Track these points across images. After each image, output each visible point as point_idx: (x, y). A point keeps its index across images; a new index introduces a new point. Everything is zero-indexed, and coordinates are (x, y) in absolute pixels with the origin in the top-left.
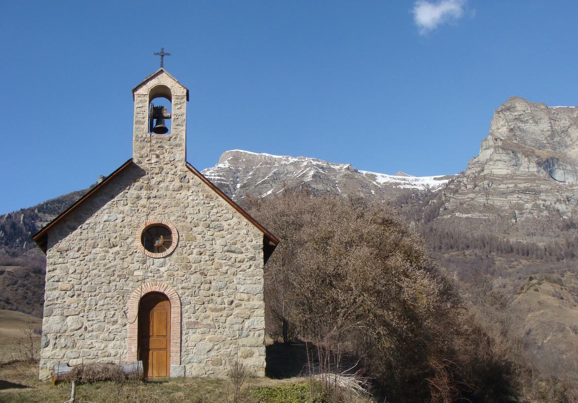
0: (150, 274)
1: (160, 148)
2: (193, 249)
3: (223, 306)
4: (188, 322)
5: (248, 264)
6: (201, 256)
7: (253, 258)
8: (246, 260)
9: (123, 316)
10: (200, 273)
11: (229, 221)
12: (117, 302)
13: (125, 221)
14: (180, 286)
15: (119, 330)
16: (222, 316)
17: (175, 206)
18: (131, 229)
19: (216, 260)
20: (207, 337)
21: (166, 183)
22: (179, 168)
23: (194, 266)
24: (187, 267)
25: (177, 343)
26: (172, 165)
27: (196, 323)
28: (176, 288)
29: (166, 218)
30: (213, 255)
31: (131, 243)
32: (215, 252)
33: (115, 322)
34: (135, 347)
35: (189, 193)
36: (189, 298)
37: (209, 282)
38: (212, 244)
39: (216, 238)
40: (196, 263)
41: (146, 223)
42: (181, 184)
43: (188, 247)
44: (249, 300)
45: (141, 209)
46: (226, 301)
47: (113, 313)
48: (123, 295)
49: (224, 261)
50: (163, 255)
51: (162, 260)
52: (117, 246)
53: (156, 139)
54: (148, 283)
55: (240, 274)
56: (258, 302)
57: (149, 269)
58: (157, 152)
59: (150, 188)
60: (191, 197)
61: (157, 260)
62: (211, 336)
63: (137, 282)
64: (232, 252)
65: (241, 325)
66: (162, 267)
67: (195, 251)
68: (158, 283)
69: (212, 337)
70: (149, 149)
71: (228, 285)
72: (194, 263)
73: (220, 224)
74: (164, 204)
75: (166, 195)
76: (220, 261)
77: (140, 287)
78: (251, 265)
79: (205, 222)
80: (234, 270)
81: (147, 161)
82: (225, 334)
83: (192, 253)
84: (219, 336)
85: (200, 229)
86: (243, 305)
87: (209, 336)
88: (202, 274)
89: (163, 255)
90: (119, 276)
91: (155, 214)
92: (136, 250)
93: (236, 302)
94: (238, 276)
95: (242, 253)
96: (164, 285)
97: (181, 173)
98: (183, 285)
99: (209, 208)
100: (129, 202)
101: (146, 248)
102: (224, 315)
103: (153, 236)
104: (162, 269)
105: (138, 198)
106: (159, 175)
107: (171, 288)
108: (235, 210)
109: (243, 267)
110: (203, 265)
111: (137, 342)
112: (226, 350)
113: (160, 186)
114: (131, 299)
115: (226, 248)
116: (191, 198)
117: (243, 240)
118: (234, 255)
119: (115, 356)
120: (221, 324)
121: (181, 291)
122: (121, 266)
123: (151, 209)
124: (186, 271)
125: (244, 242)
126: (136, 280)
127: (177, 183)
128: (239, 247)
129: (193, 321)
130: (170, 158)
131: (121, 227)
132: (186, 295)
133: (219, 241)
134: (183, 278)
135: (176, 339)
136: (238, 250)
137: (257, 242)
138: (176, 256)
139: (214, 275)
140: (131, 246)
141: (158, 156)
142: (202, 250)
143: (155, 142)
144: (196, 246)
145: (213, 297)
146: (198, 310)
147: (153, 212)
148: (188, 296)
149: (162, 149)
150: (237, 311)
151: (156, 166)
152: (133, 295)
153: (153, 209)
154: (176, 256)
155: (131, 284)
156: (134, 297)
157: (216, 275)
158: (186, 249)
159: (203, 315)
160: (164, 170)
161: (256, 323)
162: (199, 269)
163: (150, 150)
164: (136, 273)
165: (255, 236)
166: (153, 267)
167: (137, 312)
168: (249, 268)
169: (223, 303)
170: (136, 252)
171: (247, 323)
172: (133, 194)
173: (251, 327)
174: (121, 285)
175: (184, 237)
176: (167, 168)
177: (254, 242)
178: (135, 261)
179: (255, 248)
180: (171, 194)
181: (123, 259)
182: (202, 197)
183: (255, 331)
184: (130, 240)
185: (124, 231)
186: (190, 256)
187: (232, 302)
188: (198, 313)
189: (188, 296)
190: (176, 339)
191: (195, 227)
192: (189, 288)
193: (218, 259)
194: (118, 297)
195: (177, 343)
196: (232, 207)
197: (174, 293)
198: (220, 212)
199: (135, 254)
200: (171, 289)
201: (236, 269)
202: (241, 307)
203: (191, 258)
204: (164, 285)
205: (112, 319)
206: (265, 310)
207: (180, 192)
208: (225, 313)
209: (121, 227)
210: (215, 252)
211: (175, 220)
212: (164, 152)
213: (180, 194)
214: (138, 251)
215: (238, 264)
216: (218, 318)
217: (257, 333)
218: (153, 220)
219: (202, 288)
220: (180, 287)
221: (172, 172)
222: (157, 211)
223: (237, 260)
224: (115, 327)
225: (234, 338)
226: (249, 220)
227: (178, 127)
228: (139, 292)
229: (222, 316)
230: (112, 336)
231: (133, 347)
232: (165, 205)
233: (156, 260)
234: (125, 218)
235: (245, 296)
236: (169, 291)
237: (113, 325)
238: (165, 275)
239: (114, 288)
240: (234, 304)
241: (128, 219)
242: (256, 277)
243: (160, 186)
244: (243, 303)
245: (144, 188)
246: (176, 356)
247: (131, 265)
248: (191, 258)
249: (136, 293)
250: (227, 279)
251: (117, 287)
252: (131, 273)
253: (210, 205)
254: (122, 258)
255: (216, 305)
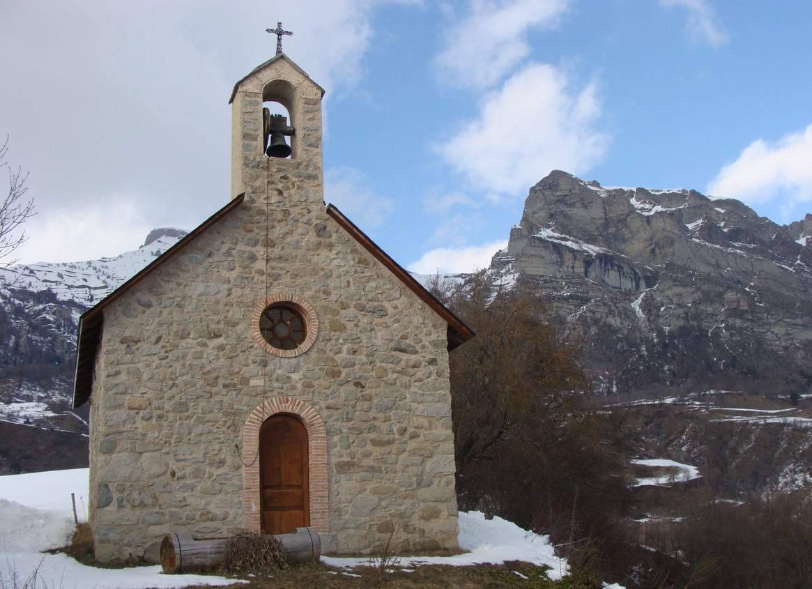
0: (276, 384)
1: (283, 180)
2: (341, 344)
3: (392, 436)
4: (339, 462)
5: (426, 370)
6: (354, 357)
7: (433, 362)
8: (423, 363)
9: (235, 452)
10: (354, 384)
11: (395, 302)
12: (224, 429)
13: (232, 296)
14: (323, 404)
15: (229, 476)
16: (389, 453)
17: (311, 275)
18: (242, 309)
19: (378, 364)
20: (369, 488)
21: (296, 237)
22: (313, 214)
23: (344, 372)
24: (334, 374)
25: (323, 497)
26: (303, 209)
27: (350, 465)
28: (317, 407)
29: (298, 293)
30: (373, 355)
31: (244, 331)
32: (376, 350)
33: (222, 463)
34: (256, 504)
35: (332, 255)
36: (339, 423)
37: (369, 398)
38: (371, 338)
39: (376, 328)
40: (348, 367)
41: (266, 300)
42: (318, 239)
43: (333, 342)
44: (430, 427)
45: (257, 277)
46: (395, 429)
47: (217, 447)
48: (234, 419)
49: (390, 365)
50: (295, 353)
51: (293, 361)
52: (221, 336)
53: (277, 164)
54: (274, 399)
55: (415, 386)
56: (444, 433)
57: (275, 376)
58: (280, 186)
59: (269, 244)
60: (336, 261)
61: (287, 361)
62: (376, 485)
63: (256, 396)
64: (401, 350)
65: (420, 467)
66: (294, 372)
67: (345, 348)
68: (290, 399)
69: (377, 487)
70: (266, 181)
71: (398, 403)
72: (344, 367)
73: (382, 306)
74: (293, 270)
75: (296, 256)
76: (384, 365)
77: (262, 405)
78: (430, 373)
79: (358, 302)
80: (405, 379)
81: (265, 199)
82: (396, 481)
83: (340, 352)
84: (387, 485)
85: (351, 311)
86: (422, 435)
87: (372, 486)
88: (357, 384)
89: (295, 353)
90: (225, 386)
91: (281, 286)
92: (252, 344)
93: (411, 430)
94: (413, 389)
95: (416, 352)
96: (299, 403)
97: (319, 221)
98: (329, 402)
99: (364, 280)
100: (237, 265)
101: (270, 341)
102: (394, 452)
103: (276, 322)
104: (295, 376)
105: (253, 258)
106: (284, 223)
107: (310, 406)
108: (404, 285)
109: (419, 375)
110: (359, 371)
111: (259, 496)
112: (398, 508)
113: (286, 242)
114: (248, 425)
115: (393, 345)
116: (335, 262)
117: (418, 333)
118: (404, 356)
119: (224, 519)
120: (389, 465)
121: (325, 413)
122: (228, 370)
123: (275, 277)
124: (333, 380)
125: (420, 336)
126: (254, 393)
127: (312, 237)
128: (412, 343)
129: (346, 461)
130: (301, 196)
131: (226, 305)
132: (333, 418)
133: (381, 334)
134: (328, 392)
135: (323, 491)
136: (411, 349)
137: (438, 337)
138: (316, 355)
139: (376, 387)
140: (243, 336)
141: (280, 193)
142: (356, 347)
143: (275, 170)
144: (347, 339)
145: (376, 423)
146: (353, 443)
147: (277, 282)
148: (337, 420)
149: (286, 181)
150: (413, 445)
151: (279, 209)
152: (251, 418)
153: (277, 277)
154: (316, 355)
155: (246, 399)
156: (251, 422)
157: (380, 386)
158: (330, 343)
159: (361, 450)
160: (292, 216)
161: (442, 464)
162: (352, 376)
163: (268, 182)
164: (253, 382)
165: (435, 326)
166: (279, 372)
167: (258, 447)
168: (428, 377)
169: (391, 431)
170: (252, 347)
171: (429, 464)
172: (244, 252)
173: (436, 471)
174: (230, 402)
175: (327, 325)
176: (294, 211)
177: (434, 337)
178: (250, 362)
179: (435, 344)
180: (304, 256)
181: (231, 358)
182: (352, 263)
183: (440, 476)
184: (240, 327)
185: (230, 312)
186: (337, 355)
187: (405, 430)
188: (353, 448)
189: (337, 420)
190: (323, 491)
191: (344, 309)
192: (338, 407)
193: (381, 362)
194: (225, 422)
195: (323, 497)
196: (398, 280)
197: (315, 416)
198: (380, 287)
199: (250, 350)
200: (311, 409)
201: (409, 378)
202: (419, 439)
203: (338, 358)
204: (299, 403)
205: (217, 458)
206: (454, 443)
207: (318, 252)
208: (394, 448)
209: (226, 305)
210: (376, 350)
211: (312, 297)
212: (291, 187)
213: (318, 255)
214: (256, 346)
215: (411, 371)
216: (385, 457)
217: (444, 479)
218: (279, 293)
219: (358, 408)
220: (323, 406)
221: (305, 219)
222: (283, 281)
223: (411, 363)
224: (221, 471)
225: (411, 489)
226: (425, 301)
227: (311, 149)
228: (260, 412)
229: (389, 453)
230: (217, 486)
231: (253, 504)
232: (295, 272)
233: (284, 361)
234: (233, 291)
235: (425, 422)
236: (308, 411)
237: (218, 467)
238: (299, 386)
239: (218, 406)
240: (407, 435)
241: (237, 292)
242: (440, 392)
243: (286, 242)
244: (422, 432)
245: (261, 243)
246: (322, 518)
247: (244, 369)
248: (338, 358)
249: (256, 415)
250: (395, 394)
251: (224, 405)
252: (245, 381)
253: (364, 275)
254: (230, 356)
255: (381, 436)
